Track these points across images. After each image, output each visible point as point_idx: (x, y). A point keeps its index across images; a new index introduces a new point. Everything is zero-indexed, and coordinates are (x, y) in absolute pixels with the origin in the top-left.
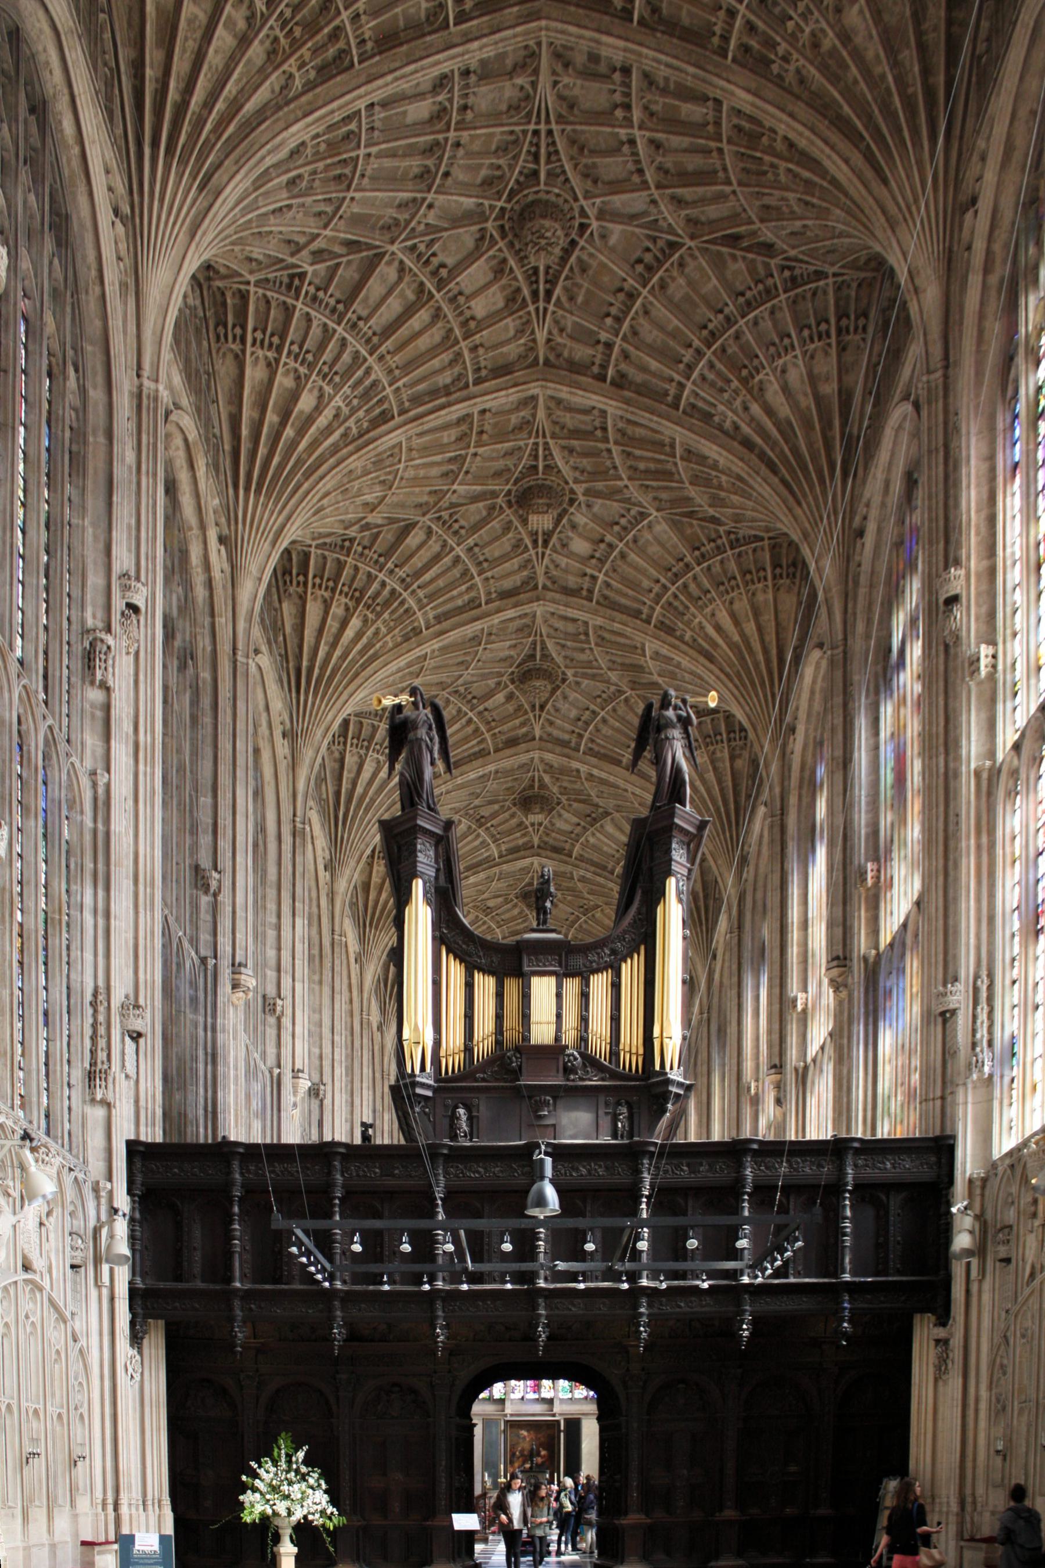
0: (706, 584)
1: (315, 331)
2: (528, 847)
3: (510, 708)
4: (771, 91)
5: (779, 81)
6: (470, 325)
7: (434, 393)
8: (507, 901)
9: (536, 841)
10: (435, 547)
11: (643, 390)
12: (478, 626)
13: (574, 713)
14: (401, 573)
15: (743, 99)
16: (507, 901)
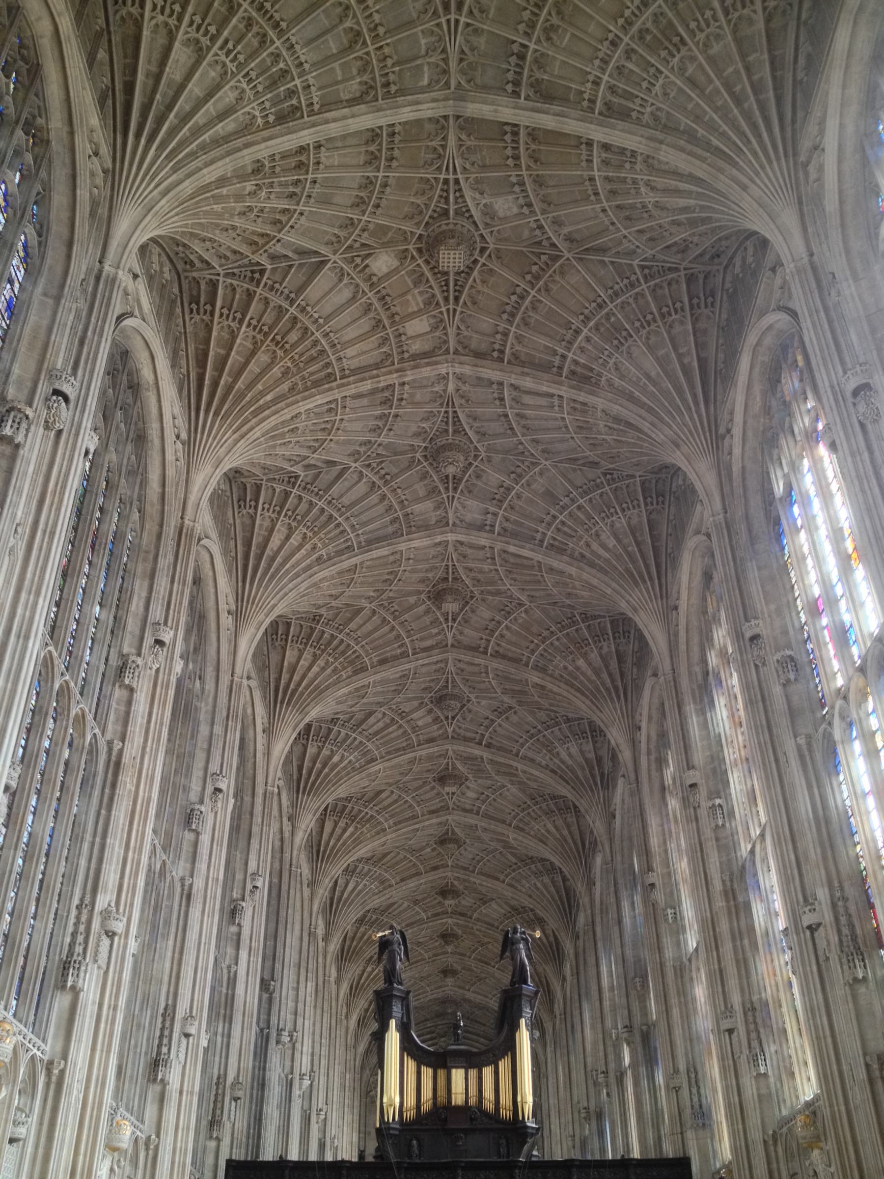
0: (539, 813)
1: (343, 734)
2: (443, 913)
3: (435, 854)
4: (548, 678)
5: (551, 676)
6: (414, 729)
7: (398, 750)
8: (431, 939)
9: (450, 910)
10: (395, 797)
11: (499, 749)
12: (417, 826)
13: (470, 856)
14: (376, 808)
15: (537, 680)
16: (431, 939)
